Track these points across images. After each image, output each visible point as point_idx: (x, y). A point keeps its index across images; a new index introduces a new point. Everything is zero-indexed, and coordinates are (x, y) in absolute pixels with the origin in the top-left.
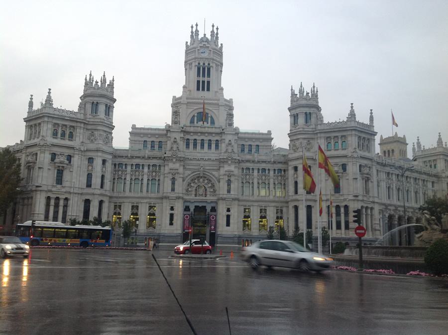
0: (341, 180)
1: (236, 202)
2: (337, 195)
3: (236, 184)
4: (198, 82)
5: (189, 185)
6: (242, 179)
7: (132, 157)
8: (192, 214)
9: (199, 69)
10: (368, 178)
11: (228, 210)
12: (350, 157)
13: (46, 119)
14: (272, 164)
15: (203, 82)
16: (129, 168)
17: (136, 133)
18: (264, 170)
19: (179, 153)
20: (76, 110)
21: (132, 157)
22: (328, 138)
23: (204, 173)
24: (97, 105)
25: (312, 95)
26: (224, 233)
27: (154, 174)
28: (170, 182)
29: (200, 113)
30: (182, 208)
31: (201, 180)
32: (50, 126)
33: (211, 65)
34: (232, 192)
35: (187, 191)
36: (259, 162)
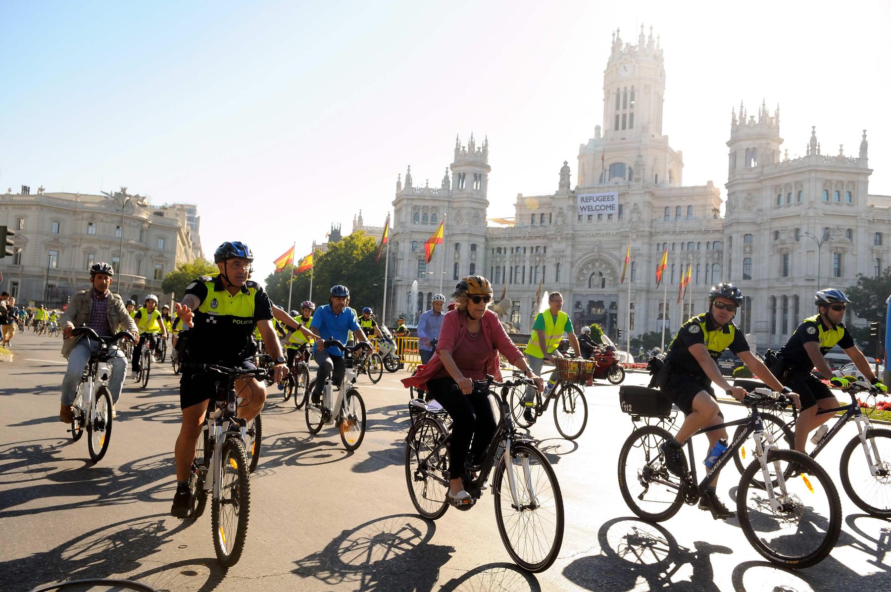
0: (790, 256)
1: (644, 295)
2: (784, 279)
3: (645, 268)
4: (617, 117)
7: (510, 239)
8: (584, 312)
10: (841, 248)
11: (632, 306)
12: (804, 216)
13: (405, 202)
14: (704, 234)
15: (624, 116)
16: (508, 252)
17: (521, 203)
19: (566, 228)
20: (441, 188)
23: (601, 254)
25: (760, 120)
27: (538, 259)
28: (554, 269)
29: (614, 164)
30: (571, 304)
31: (597, 264)
32: (409, 210)
33: (636, 88)
34: (636, 281)
36: (681, 233)
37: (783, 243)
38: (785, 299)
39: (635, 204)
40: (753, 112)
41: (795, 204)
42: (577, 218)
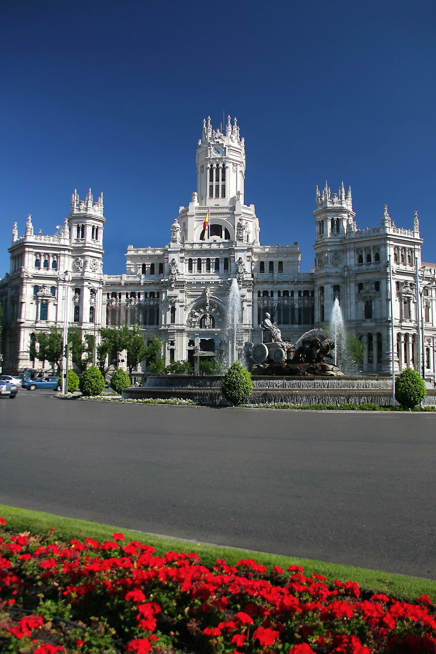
2: (368, 320)
4: (211, 187)
10: (408, 297)
12: (383, 272)
14: (296, 284)
15: (217, 186)
18: (286, 293)
21: (126, 284)
22: (357, 249)
31: (207, 308)
33: (226, 165)
34: (244, 322)
35: (190, 322)
36: (278, 283)
37: (368, 292)
39: (240, 258)
41: (373, 263)
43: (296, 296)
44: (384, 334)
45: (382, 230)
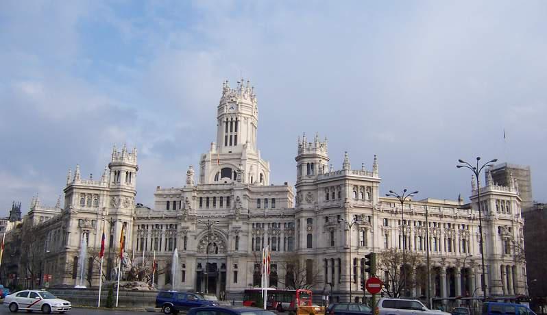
4: (226, 136)
5: (201, 242)
6: (253, 235)
9: (227, 123)
11: (236, 267)
13: (75, 190)
15: (231, 136)
16: (150, 228)
24: (119, 174)
26: (231, 289)
28: (183, 241)
31: (212, 237)
32: (77, 196)
33: (239, 118)
34: (239, 249)
35: (199, 247)
36: (269, 216)
38: (333, 260)
40: (309, 139)
42: (199, 205)
43: (282, 227)
44: (342, 260)
45: (343, 172)
